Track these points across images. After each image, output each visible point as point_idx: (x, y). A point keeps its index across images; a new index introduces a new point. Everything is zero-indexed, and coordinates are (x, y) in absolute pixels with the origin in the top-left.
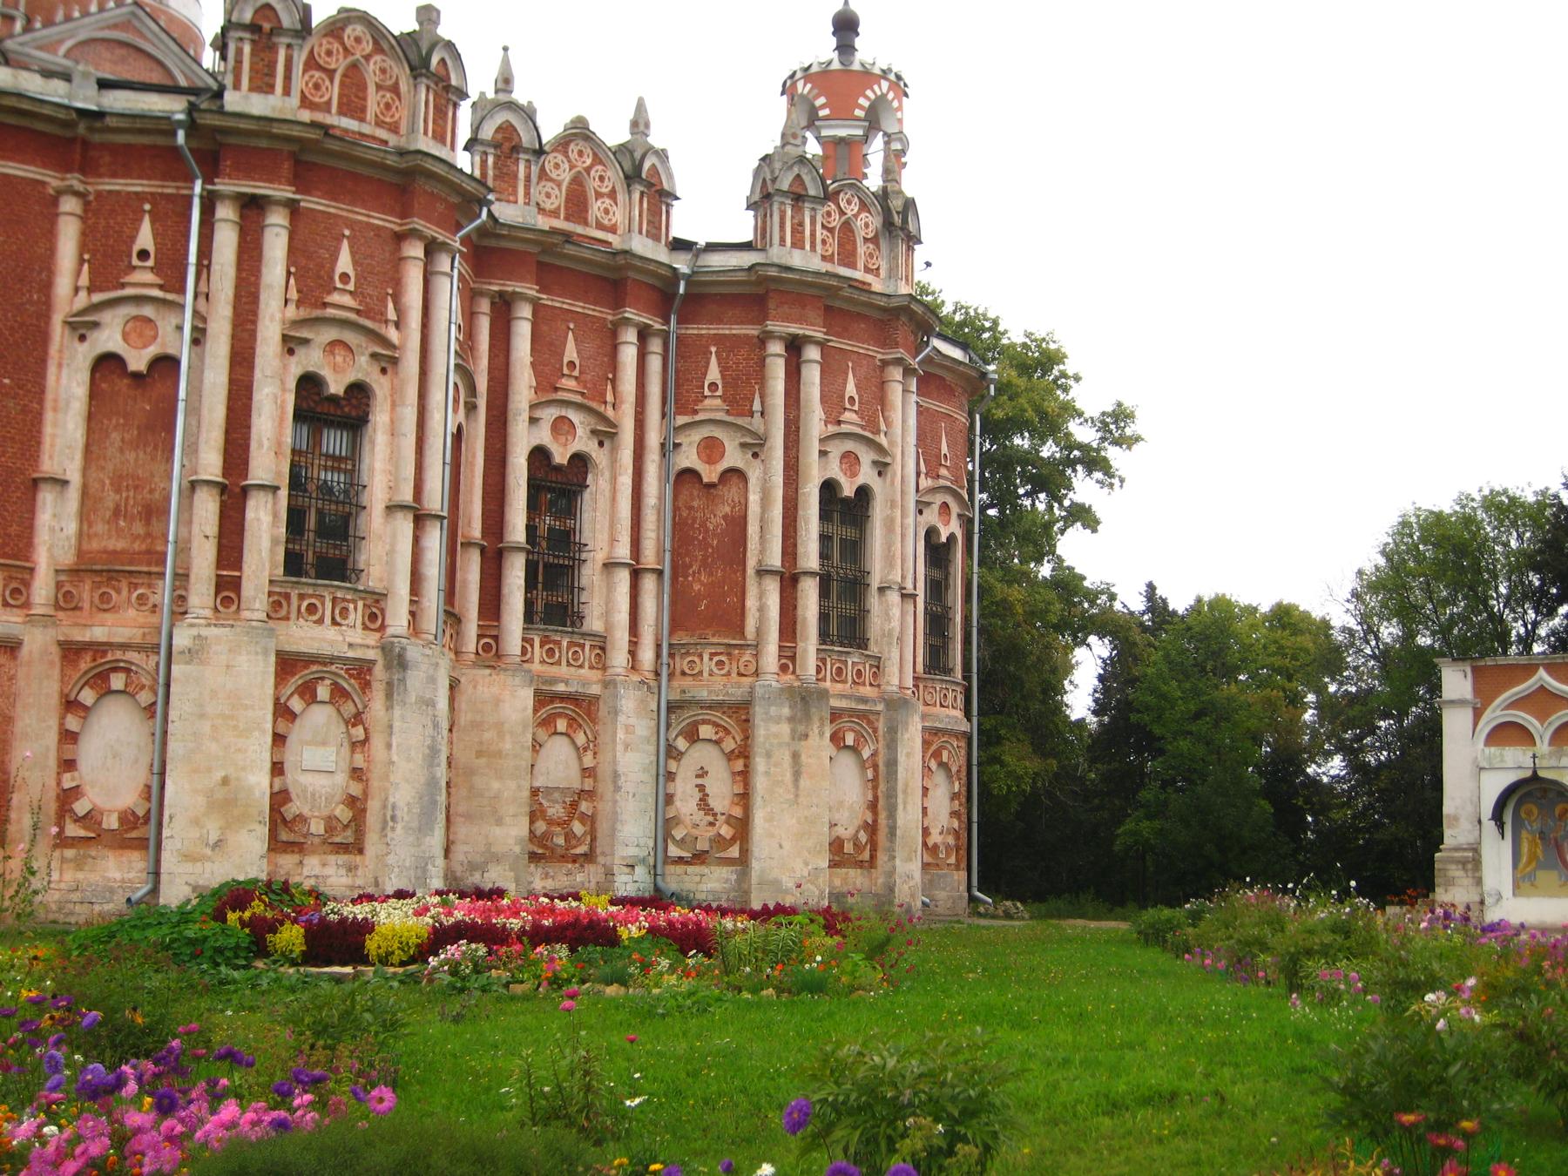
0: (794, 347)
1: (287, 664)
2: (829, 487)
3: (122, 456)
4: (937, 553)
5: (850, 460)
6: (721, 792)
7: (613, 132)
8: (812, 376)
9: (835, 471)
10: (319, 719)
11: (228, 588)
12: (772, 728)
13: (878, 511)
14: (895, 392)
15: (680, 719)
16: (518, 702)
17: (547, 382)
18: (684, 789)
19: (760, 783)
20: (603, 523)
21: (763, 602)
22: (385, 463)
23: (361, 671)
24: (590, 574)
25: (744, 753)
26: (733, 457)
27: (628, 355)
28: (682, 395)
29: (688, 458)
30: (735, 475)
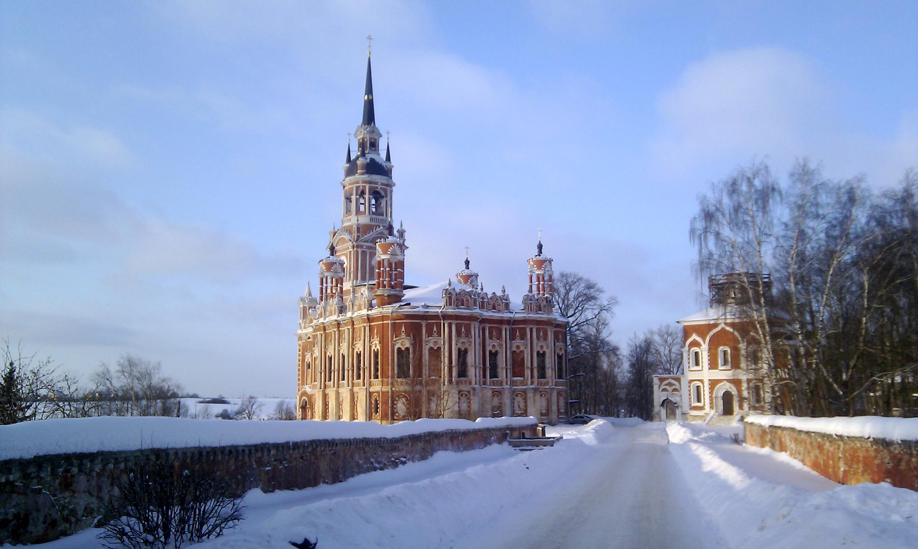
0: (531, 330)
1: (459, 392)
2: (538, 352)
3: (433, 363)
4: (560, 357)
5: (542, 347)
6: (522, 405)
7: (499, 293)
8: (534, 333)
9: (539, 349)
10: (463, 399)
11: (450, 381)
12: (530, 395)
13: (547, 355)
14: (549, 333)
15: (514, 394)
16: (489, 393)
17: (491, 338)
18: (516, 405)
19: (529, 404)
20: (501, 361)
21: (528, 373)
22: (470, 359)
23: (469, 392)
24: (499, 370)
25: (525, 399)
26: (522, 348)
27: (504, 332)
28: (513, 338)
29: (514, 349)
30: (522, 352)
